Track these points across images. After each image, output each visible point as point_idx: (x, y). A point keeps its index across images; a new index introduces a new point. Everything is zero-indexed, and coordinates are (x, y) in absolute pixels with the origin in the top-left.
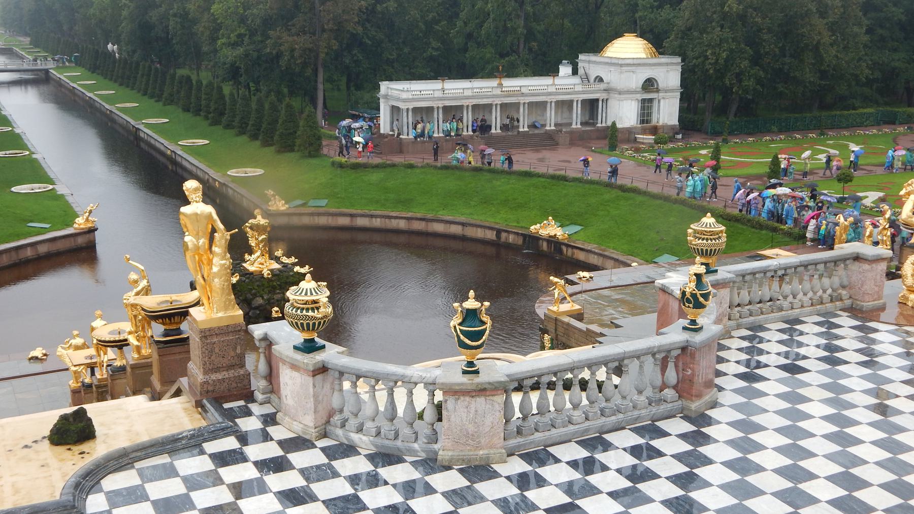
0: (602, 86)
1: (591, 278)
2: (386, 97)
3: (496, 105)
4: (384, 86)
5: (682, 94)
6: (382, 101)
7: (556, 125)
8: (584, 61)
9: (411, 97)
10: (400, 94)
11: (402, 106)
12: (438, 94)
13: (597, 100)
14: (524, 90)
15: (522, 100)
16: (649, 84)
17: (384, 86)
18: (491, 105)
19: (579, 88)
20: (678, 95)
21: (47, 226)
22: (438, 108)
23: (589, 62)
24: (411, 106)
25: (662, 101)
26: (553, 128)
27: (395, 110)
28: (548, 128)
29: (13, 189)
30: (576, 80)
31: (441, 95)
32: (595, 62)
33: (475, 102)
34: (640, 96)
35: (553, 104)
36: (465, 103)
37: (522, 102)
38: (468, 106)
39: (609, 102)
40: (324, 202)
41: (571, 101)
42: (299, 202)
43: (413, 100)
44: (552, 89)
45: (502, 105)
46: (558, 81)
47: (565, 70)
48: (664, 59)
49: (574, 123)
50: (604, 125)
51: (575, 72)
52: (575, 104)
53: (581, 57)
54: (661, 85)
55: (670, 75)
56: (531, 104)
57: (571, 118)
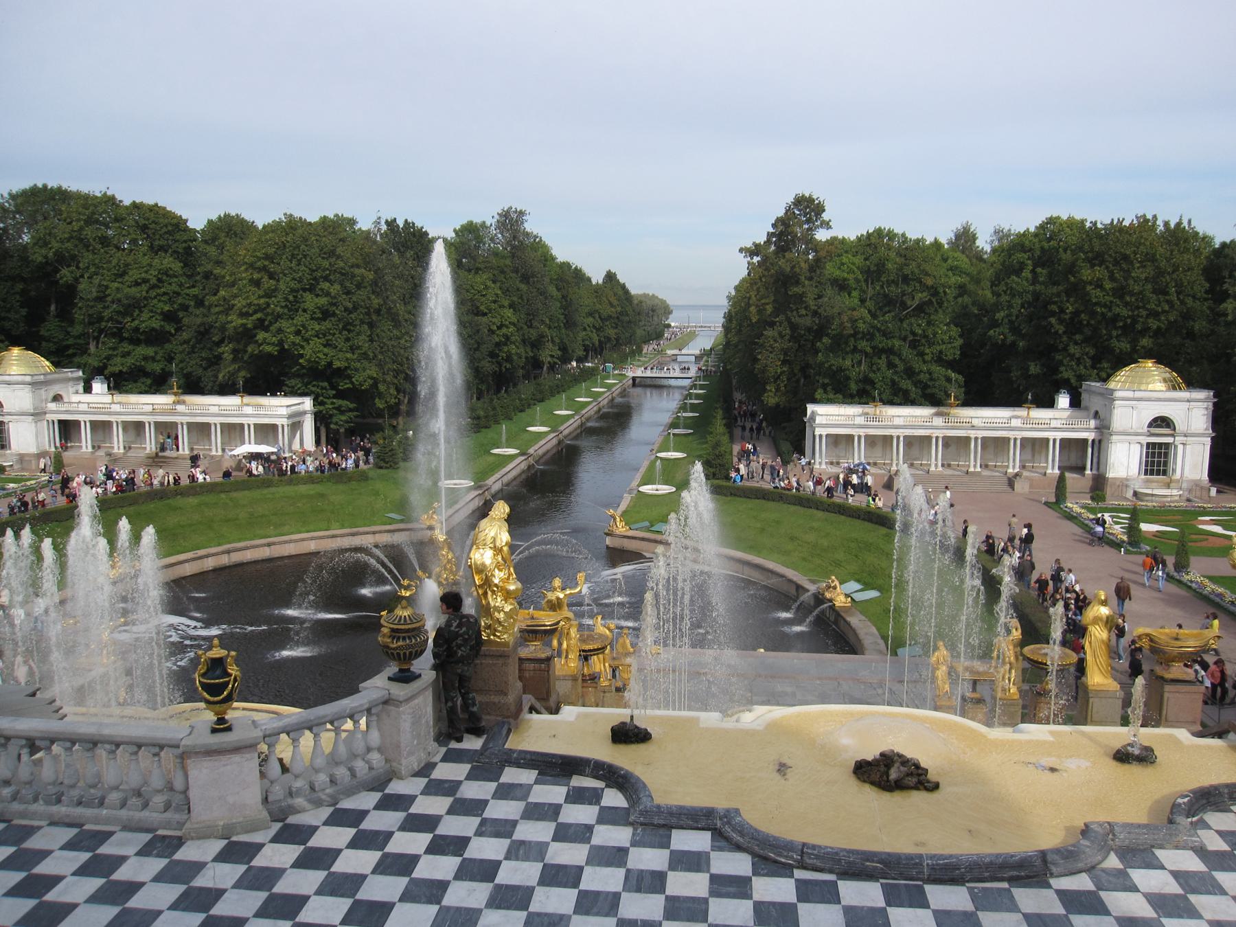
3: (937, 438)
4: (811, 408)
5: (1212, 439)
10: (827, 417)
12: (860, 420)
13: (1085, 441)
14: (975, 422)
17: (811, 408)
18: (929, 438)
20: (1208, 441)
22: (859, 437)
24: (824, 434)
25: (1180, 448)
42: (647, 524)
44: (1016, 423)
45: (944, 438)
46: (1040, 414)
47: (1063, 400)
48: (1185, 394)
51: (1075, 403)
54: (1180, 426)
56: (985, 440)
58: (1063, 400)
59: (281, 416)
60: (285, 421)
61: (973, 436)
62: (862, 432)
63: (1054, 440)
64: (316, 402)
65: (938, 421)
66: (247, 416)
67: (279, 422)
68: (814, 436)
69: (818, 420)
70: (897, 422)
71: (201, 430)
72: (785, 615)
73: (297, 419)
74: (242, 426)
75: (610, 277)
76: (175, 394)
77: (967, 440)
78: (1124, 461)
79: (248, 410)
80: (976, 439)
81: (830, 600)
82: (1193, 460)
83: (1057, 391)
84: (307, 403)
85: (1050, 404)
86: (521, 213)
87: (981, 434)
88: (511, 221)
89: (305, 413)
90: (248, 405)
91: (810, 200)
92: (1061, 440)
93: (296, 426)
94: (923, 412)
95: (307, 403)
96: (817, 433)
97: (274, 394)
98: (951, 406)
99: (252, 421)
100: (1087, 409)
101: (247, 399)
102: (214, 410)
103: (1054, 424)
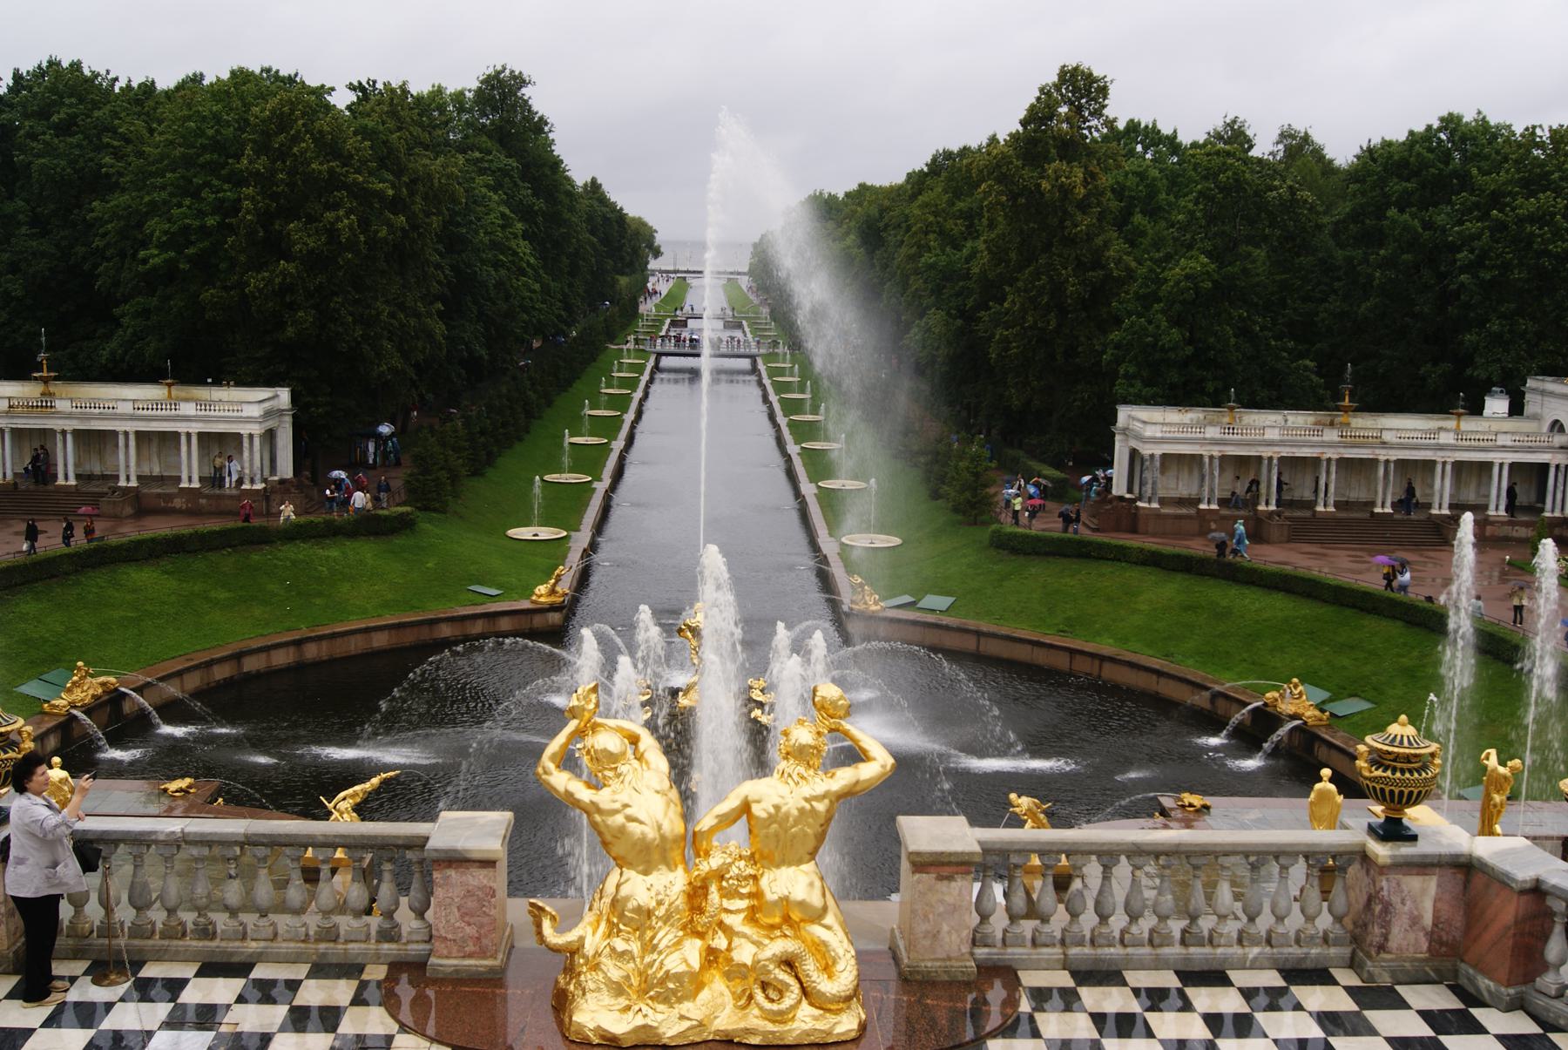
0: (1558, 440)
1: (1206, 807)
2: (1125, 431)
3: (1329, 460)
6: (1117, 438)
7: (1451, 507)
8: (1534, 390)
9: (1159, 435)
11: (1146, 450)
12: (1212, 432)
14: (1387, 437)
15: (1382, 455)
17: (1124, 414)
21: (494, 592)
23: (1543, 393)
26: (1446, 512)
27: (1134, 454)
28: (1435, 511)
29: (512, 532)
30: (1515, 424)
31: (1218, 436)
32: (1552, 394)
33: (1286, 452)
35: (1449, 468)
37: (1382, 458)
38: (1270, 459)
40: (942, 602)
41: (1487, 466)
42: (908, 599)
43: (1162, 441)
44: (1446, 438)
46: (1469, 424)
47: (1497, 405)
49: (1492, 506)
50: (1557, 514)
51: (1516, 409)
52: (1439, 468)
53: (1530, 383)
57: (1488, 496)
58: (1497, 405)
59: (249, 420)
60: (256, 429)
61: (1382, 458)
62: (1216, 451)
63: (1501, 465)
64: (295, 399)
65: (1331, 435)
66: (186, 419)
67: (244, 430)
70: (1272, 435)
71: (94, 441)
72: (1214, 741)
73: (270, 424)
74: (176, 435)
75: (594, 186)
76: (45, 381)
77: (1373, 463)
79: (188, 409)
80: (1387, 462)
81: (1294, 717)
83: (1488, 391)
84: (284, 395)
85: (1477, 409)
86: (520, 81)
87: (1395, 455)
88: (502, 92)
89: (281, 412)
90: (187, 400)
91: (1089, 78)
92: (1512, 465)
93: (270, 436)
94: (1299, 420)
97: (217, 383)
98: (1346, 410)
99: (195, 428)
100: (1536, 417)
101: (177, 391)
102: (127, 408)
103: (1503, 440)
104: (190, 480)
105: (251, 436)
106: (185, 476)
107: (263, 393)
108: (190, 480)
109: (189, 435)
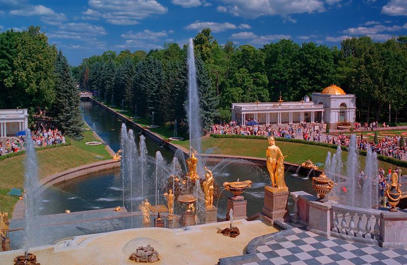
4: (234, 105)
12: (256, 109)
16: (343, 105)
17: (234, 105)
19: (313, 107)
20: (355, 110)
24: (245, 113)
34: (339, 111)
36: (267, 112)
39: (327, 112)
44: (302, 107)
46: (304, 104)
48: (348, 96)
51: (311, 100)
55: (350, 101)
58: (308, 100)
62: (257, 112)
68: (241, 115)
69: (243, 109)
70: (268, 108)
78: (334, 118)
82: (351, 116)
84: (26, 111)
87: (292, 111)
95: (26, 111)
96: (243, 113)
104: (4, 136)
105: (22, 123)
106: (2, 135)
107: (20, 111)
108: (4, 136)
109: (3, 123)
